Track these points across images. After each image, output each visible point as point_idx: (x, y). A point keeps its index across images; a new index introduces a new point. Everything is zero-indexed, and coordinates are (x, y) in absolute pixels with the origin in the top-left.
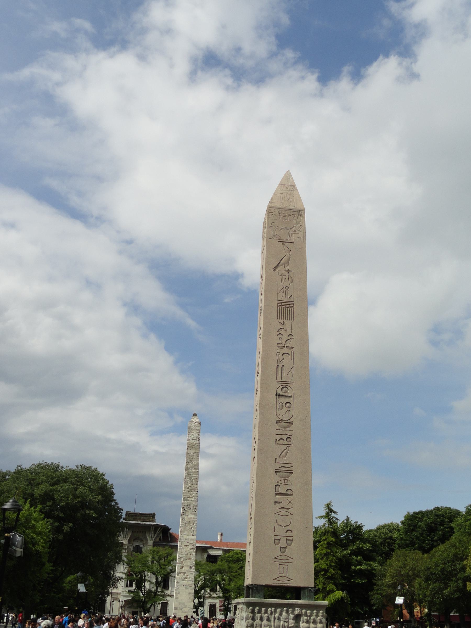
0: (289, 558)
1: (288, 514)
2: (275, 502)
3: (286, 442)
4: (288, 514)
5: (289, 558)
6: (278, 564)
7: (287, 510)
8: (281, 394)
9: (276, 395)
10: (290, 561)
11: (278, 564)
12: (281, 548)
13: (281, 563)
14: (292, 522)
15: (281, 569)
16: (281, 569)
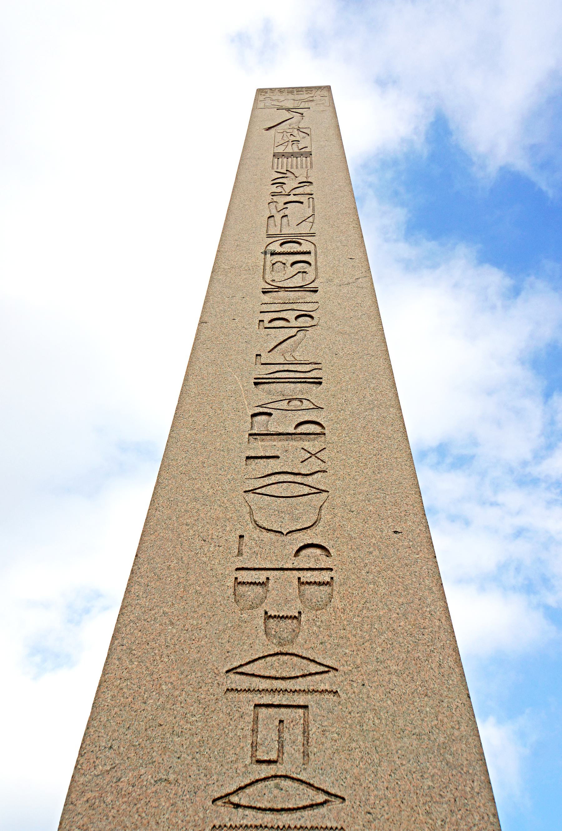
0: (314, 668)
1: (307, 490)
2: (248, 458)
3: (293, 323)
4: (307, 490)
5: (314, 668)
6: (246, 703)
7: (299, 479)
8: (279, 249)
9: (265, 253)
10: (324, 682)
11: (246, 703)
12: (268, 617)
13: (267, 699)
14: (326, 516)
15: (268, 734)
16: (268, 734)
